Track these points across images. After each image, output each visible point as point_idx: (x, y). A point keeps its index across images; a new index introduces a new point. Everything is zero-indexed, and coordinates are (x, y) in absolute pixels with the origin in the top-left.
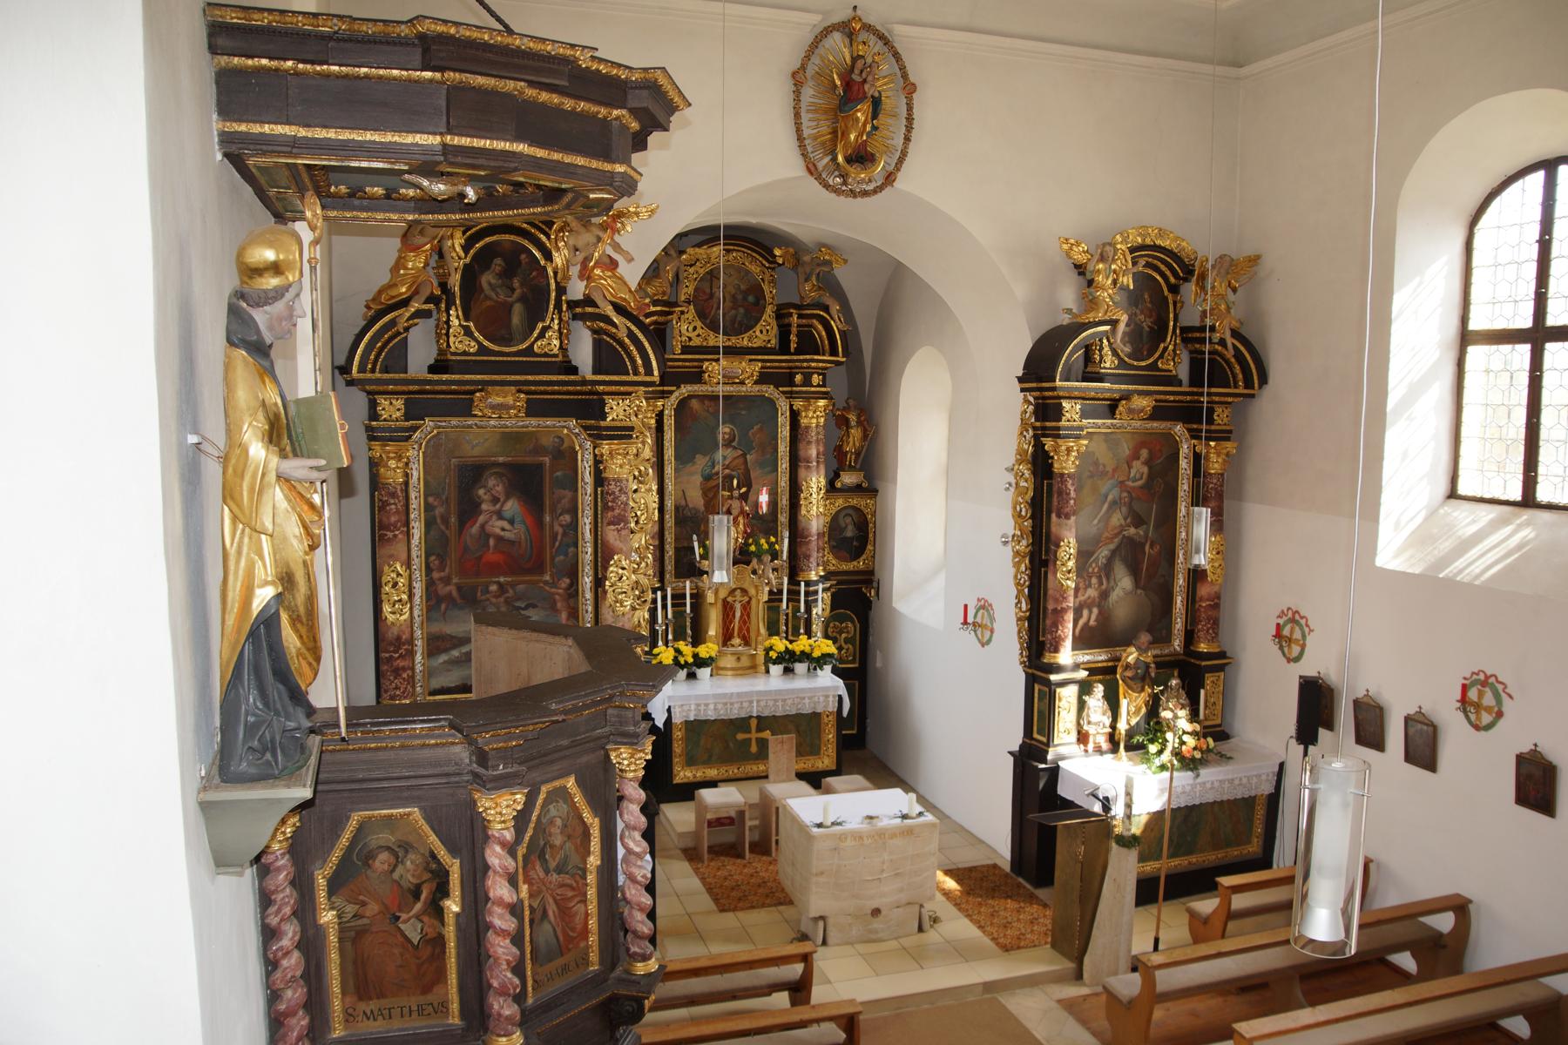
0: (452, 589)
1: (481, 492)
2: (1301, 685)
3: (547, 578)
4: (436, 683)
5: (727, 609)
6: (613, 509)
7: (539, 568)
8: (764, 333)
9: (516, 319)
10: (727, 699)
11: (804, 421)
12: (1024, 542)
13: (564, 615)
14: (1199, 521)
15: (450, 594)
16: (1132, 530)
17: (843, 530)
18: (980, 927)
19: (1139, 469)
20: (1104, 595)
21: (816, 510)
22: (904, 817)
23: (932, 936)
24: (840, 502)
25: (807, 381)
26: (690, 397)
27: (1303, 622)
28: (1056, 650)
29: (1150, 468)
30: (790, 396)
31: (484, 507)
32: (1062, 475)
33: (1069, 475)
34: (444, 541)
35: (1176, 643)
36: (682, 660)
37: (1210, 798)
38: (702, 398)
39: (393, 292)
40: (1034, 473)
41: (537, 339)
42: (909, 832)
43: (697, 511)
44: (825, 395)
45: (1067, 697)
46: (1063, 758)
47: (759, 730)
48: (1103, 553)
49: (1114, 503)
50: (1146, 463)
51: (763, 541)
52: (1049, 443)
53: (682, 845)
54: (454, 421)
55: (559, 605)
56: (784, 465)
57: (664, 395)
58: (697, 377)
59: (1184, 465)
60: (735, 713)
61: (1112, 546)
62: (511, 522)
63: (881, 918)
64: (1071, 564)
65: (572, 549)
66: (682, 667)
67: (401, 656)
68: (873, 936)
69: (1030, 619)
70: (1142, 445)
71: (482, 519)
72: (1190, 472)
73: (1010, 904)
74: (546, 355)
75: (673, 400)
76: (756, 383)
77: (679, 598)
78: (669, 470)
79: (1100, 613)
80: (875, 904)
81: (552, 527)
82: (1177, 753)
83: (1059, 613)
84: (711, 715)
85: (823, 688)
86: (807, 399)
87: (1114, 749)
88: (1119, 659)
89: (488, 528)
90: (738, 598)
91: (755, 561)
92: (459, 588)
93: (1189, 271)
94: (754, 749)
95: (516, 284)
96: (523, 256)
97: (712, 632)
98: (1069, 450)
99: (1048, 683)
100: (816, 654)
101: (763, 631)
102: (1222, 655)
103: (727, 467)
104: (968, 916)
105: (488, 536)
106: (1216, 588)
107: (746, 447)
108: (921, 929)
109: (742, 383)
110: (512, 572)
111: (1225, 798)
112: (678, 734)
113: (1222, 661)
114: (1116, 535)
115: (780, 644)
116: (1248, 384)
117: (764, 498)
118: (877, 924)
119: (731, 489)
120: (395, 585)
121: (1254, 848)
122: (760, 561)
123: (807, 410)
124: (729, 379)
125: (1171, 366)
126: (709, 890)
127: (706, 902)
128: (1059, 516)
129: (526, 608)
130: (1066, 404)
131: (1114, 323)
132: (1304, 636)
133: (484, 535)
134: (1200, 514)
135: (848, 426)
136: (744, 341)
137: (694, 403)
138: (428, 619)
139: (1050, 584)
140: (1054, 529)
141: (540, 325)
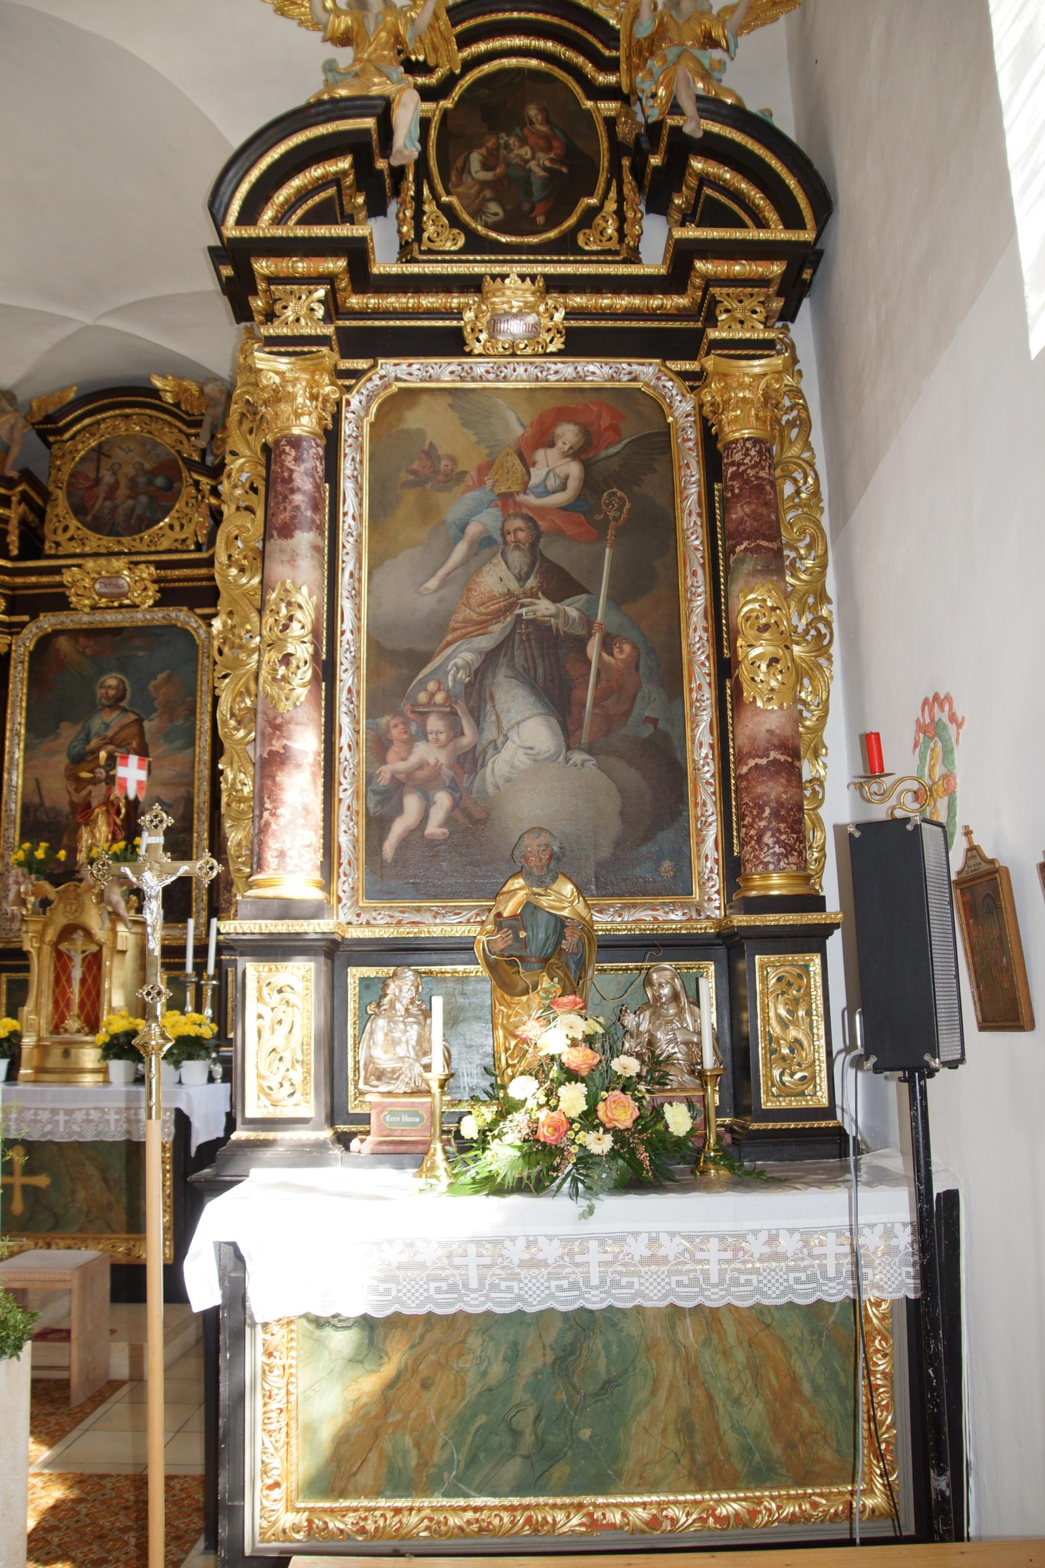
16: (544, 607)
19: (556, 470)
26: (56, 633)
29: (587, 466)
33: (296, 442)
38: (74, 634)
48: (460, 658)
49: (485, 542)
50: (576, 454)
61: (485, 643)
70: (562, 415)
79: (456, 805)
107: (144, 708)
114: (497, 616)
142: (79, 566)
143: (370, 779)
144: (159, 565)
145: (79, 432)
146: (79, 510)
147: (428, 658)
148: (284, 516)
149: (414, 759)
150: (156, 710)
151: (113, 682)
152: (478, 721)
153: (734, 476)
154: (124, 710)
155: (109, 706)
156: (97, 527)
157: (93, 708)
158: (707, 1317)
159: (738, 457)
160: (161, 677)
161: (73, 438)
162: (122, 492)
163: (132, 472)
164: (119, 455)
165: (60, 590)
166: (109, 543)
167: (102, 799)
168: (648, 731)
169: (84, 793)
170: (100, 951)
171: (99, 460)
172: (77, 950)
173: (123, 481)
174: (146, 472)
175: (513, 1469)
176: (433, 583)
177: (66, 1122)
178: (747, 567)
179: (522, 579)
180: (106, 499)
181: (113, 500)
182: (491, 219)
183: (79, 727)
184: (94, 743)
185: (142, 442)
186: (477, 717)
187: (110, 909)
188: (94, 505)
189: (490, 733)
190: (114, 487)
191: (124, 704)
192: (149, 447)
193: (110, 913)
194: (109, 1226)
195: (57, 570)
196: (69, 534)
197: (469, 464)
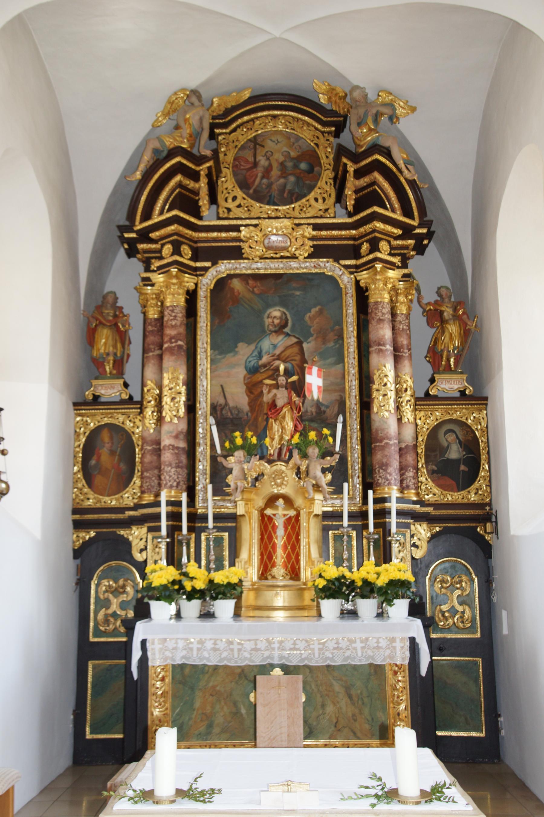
5: (266, 525)
8: (319, 202)
17: (444, 450)
24: (438, 415)
25: (374, 248)
26: (230, 277)
36: (188, 585)
38: (244, 277)
43: (239, 410)
51: (312, 435)
75: (208, 281)
76: (310, 256)
91: (296, 453)
97: (244, 555)
100: (381, 582)
103: (279, 358)
107: (302, 334)
109: (294, 257)
112: (157, 686)
122: (304, 456)
123: (374, 281)
124: (276, 253)
135: (443, 321)
137: (236, 284)
144: (316, 227)
145: (238, 126)
146: (244, 185)
150: (312, 335)
151: (277, 314)
154: (287, 335)
155: (276, 332)
156: (258, 197)
157: (263, 333)
160: (314, 311)
161: (235, 130)
162: (275, 172)
163: (281, 159)
164: (270, 145)
165: (238, 244)
166: (269, 209)
167: (286, 400)
169: (271, 395)
170: (298, 515)
172: (280, 514)
174: (292, 159)
177: (320, 649)
180: (263, 177)
181: (268, 178)
183: (252, 347)
185: (288, 136)
187: (314, 482)
188: (254, 181)
190: (268, 170)
191: (287, 330)
192: (292, 140)
193: (313, 485)
194: (355, 733)
195: (236, 228)
196: (237, 203)
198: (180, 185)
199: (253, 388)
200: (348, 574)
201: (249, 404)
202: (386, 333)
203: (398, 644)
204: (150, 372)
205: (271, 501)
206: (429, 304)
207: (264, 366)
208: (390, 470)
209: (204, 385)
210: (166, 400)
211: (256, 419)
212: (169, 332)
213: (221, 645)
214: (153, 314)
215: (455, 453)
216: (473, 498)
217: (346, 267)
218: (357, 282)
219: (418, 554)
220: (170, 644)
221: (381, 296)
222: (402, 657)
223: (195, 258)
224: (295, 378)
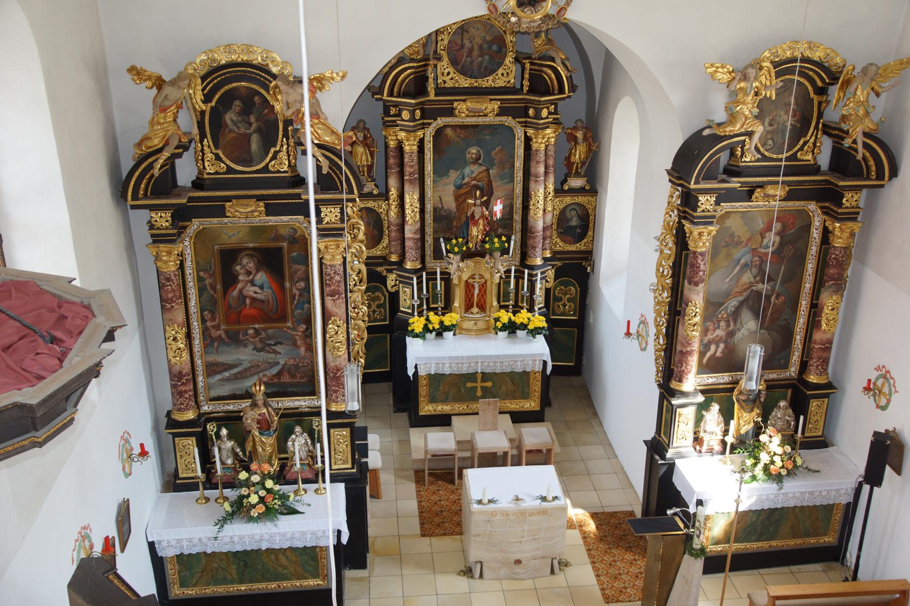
0: (221, 332)
1: (238, 268)
2: (873, 444)
3: (289, 324)
4: (214, 393)
5: (469, 287)
6: (330, 286)
7: (283, 318)
9: (255, 144)
10: (459, 360)
11: (535, 146)
12: (665, 295)
13: (303, 349)
14: (754, 357)
15: (220, 336)
17: (569, 220)
18: (598, 576)
19: (772, 239)
20: (731, 334)
21: (544, 207)
22: (544, 499)
23: (560, 579)
24: (568, 200)
25: (538, 116)
26: (445, 127)
27: (892, 381)
28: (680, 381)
29: (782, 238)
30: (526, 125)
31: (241, 278)
32: (695, 253)
33: (702, 254)
34: (214, 302)
35: (793, 369)
36: (431, 327)
37: (791, 504)
38: (454, 127)
39: (150, 144)
40: (676, 244)
41: (271, 161)
42: (544, 512)
43: (450, 211)
44: (556, 122)
45: (685, 417)
46: (681, 456)
47: (483, 380)
48: (733, 303)
50: (778, 234)
51: (496, 240)
52: (687, 226)
53: (416, 467)
54: (215, 220)
55: (299, 343)
56: (519, 175)
57: (423, 126)
58: (450, 112)
59: (816, 234)
60: (465, 370)
61: (741, 298)
62: (261, 287)
63: (521, 566)
64: (697, 319)
65: (306, 305)
66: (431, 332)
67: (183, 384)
68: (516, 577)
69: (665, 350)
71: (239, 286)
72: (818, 241)
73: (629, 556)
74: (279, 172)
76: (497, 115)
77: (432, 276)
78: (429, 181)
79: (726, 347)
80: (517, 557)
81: (291, 290)
82: (766, 468)
83: (685, 354)
84: (447, 371)
85: (537, 350)
86: (537, 129)
87: (723, 452)
88: (736, 382)
89: (245, 292)
90: (477, 280)
91: (488, 257)
92: (226, 332)
93: (834, 78)
94: (479, 393)
95: (252, 119)
96: (256, 98)
97: (456, 304)
98: (700, 234)
99: (672, 405)
100: (531, 327)
101: (495, 303)
102: (829, 386)
104: (593, 563)
105: (245, 297)
106: (828, 336)
107: (490, 163)
108: (552, 572)
109: (486, 115)
110: (264, 322)
111: (805, 504)
113: (828, 389)
115: (505, 316)
116: (880, 176)
117: (498, 208)
118: (518, 569)
119: (476, 198)
120: (175, 339)
121: (829, 539)
122: (491, 255)
125: (809, 157)
126: (421, 513)
127: (415, 525)
128: (690, 283)
129: (275, 345)
130: (702, 198)
131: (750, 134)
132: (890, 394)
133: (242, 297)
134: (755, 352)
135: (576, 143)
136: (488, 82)
137: (449, 131)
138: (206, 353)
139: (680, 332)
140: (686, 292)
141: (273, 150)
142: (464, 101)
143: (701, 341)
146: (454, 62)
147: (724, 303)
148: (697, 279)
149: (715, 335)
151: (474, 151)
152: (735, 321)
153: (834, 258)
154: (480, 165)
156: (464, 72)
157: (465, 164)
158: (802, 507)
159: (837, 253)
162: (476, 53)
163: (480, 42)
164: (473, 31)
168: (784, 323)
170: (486, 282)
171: (462, 34)
173: (476, 47)
175: (754, 537)
176: (727, 280)
178: (831, 289)
179: (755, 277)
180: (467, 57)
181: (471, 57)
182: (769, 147)
183: (459, 172)
184: (466, 180)
186: (735, 321)
189: (738, 325)
190: (471, 50)
191: (480, 162)
196: (450, 77)
197: (744, 239)
198: (415, 73)
199: (460, 198)
200: (513, 318)
201: (458, 207)
202: (541, 169)
203: (537, 362)
204: (393, 183)
205: (472, 277)
206: (568, 128)
207: (466, 184)
208: (537, 250)
209: (429, 193)
210: (408, 211)
211: (460, 216)
212: (408, 170)
213: (453, 365)
214: (392, 144)
215: (574, 222)
216: (583, 248)
217: (520, 122)
218: (526, 133)
219: (549, 285)
220: (428, 365)
221: (539, 144)
222: (538, 367)
223: (422, 117)
224: (485, 198)
